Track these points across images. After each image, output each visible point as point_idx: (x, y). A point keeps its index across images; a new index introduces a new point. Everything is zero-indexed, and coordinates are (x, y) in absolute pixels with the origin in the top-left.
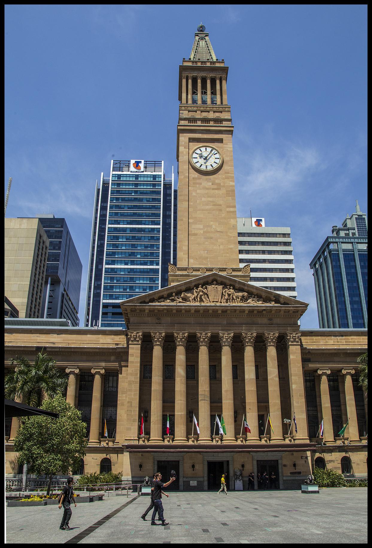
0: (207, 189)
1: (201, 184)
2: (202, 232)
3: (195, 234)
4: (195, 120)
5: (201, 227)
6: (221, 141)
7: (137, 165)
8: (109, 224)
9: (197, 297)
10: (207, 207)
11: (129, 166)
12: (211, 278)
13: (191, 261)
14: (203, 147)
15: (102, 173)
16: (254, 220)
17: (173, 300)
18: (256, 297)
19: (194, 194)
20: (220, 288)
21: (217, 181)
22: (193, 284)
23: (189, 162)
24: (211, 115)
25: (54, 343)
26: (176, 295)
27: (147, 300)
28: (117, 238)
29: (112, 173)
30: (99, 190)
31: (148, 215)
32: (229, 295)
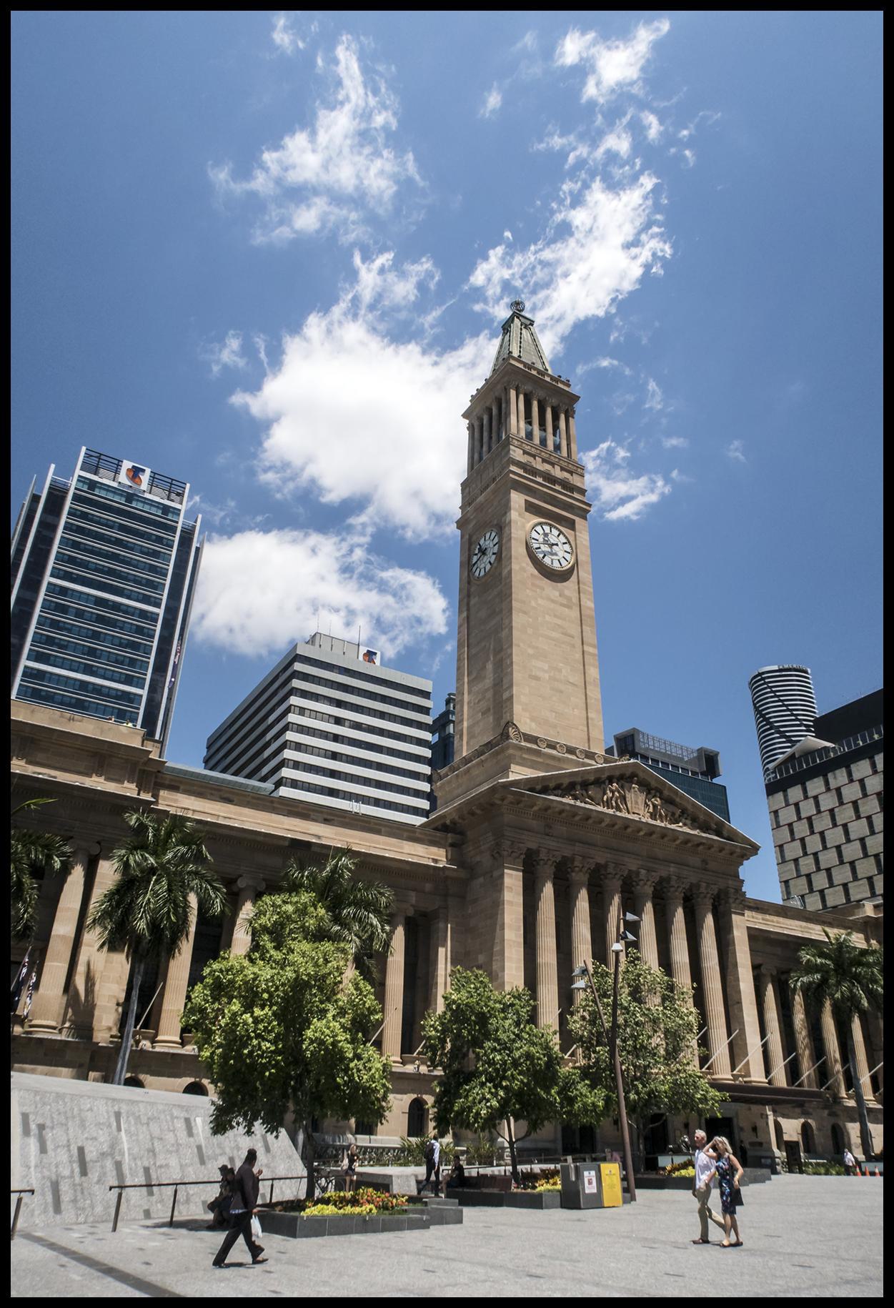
0: (553, 601)
2: (547, 676)
3: (537, 678)
4: (534, 472)
7: (135, 473)
8: (52, 575)
10: (554, 634)
11: (117, 472)
15: (53, 466)
16: (363, 650)
25: (319, 837)
27: (539, 787)
28: (63, 609)
29: (78, 472)
30: (35, 499)
31: (137, 581)
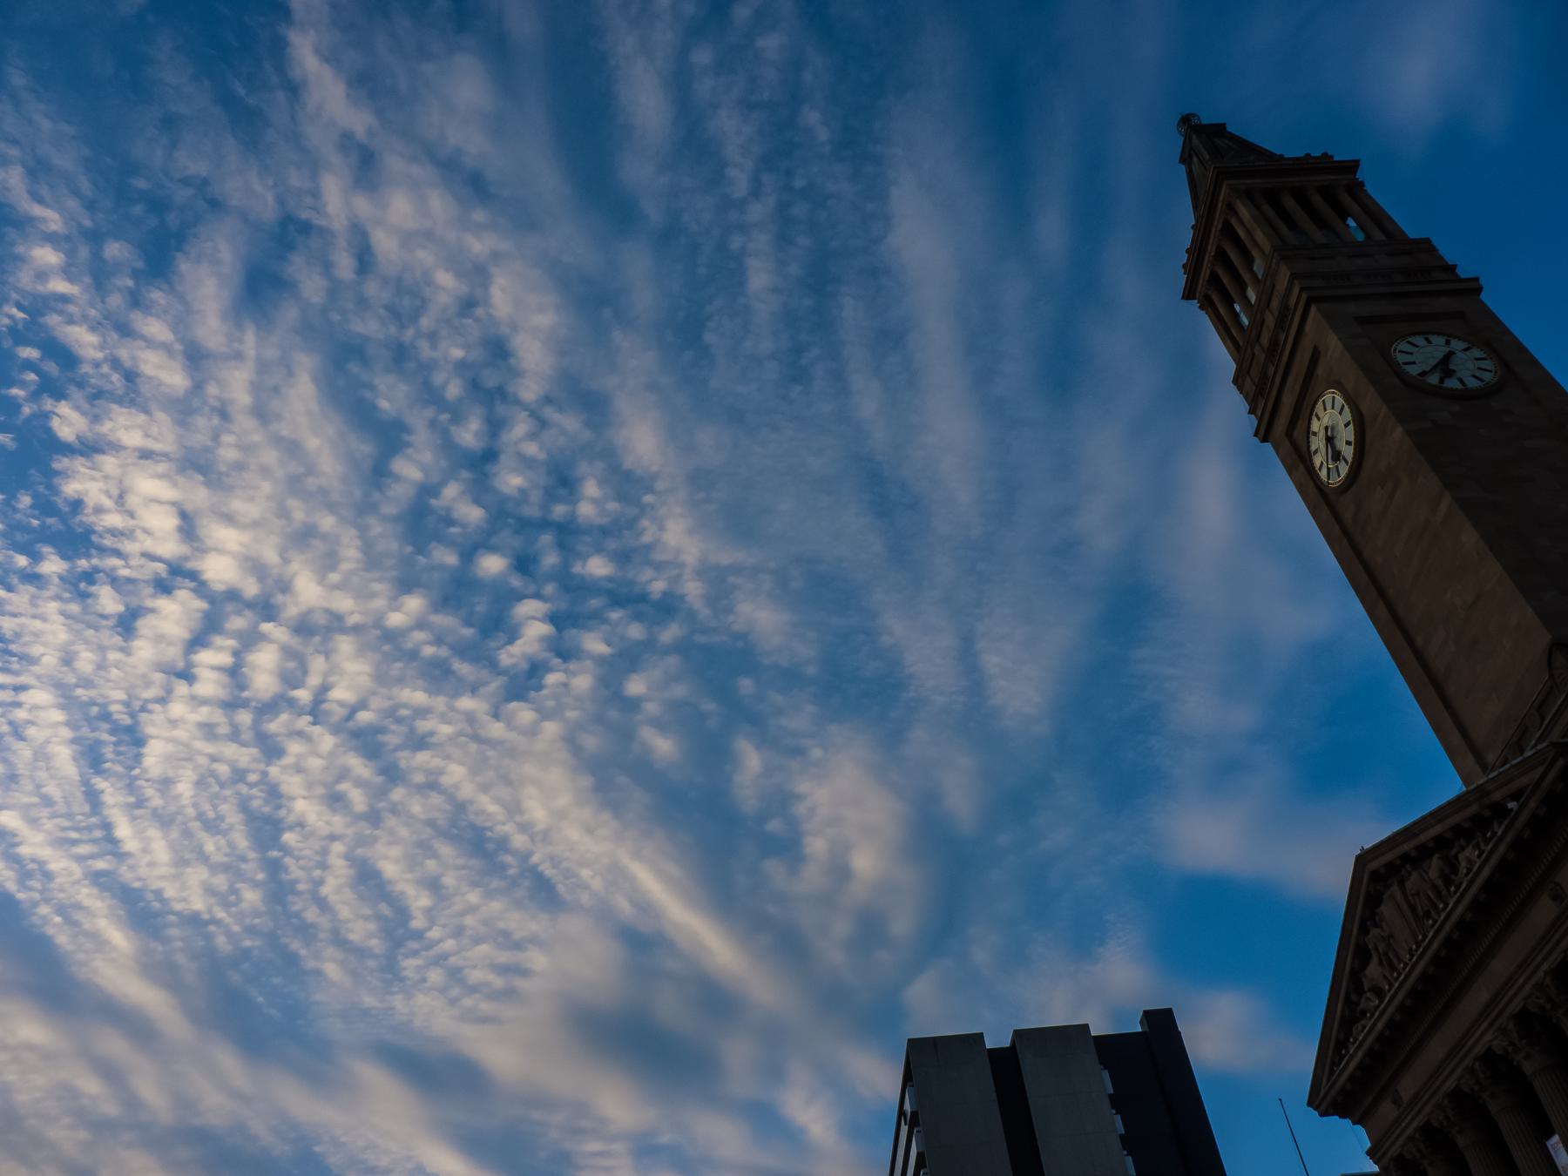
6: (1316, 356)
14: (1310, 419)
17: (1364, 1013)
20: (1395, 889)
24: (1270, 321)
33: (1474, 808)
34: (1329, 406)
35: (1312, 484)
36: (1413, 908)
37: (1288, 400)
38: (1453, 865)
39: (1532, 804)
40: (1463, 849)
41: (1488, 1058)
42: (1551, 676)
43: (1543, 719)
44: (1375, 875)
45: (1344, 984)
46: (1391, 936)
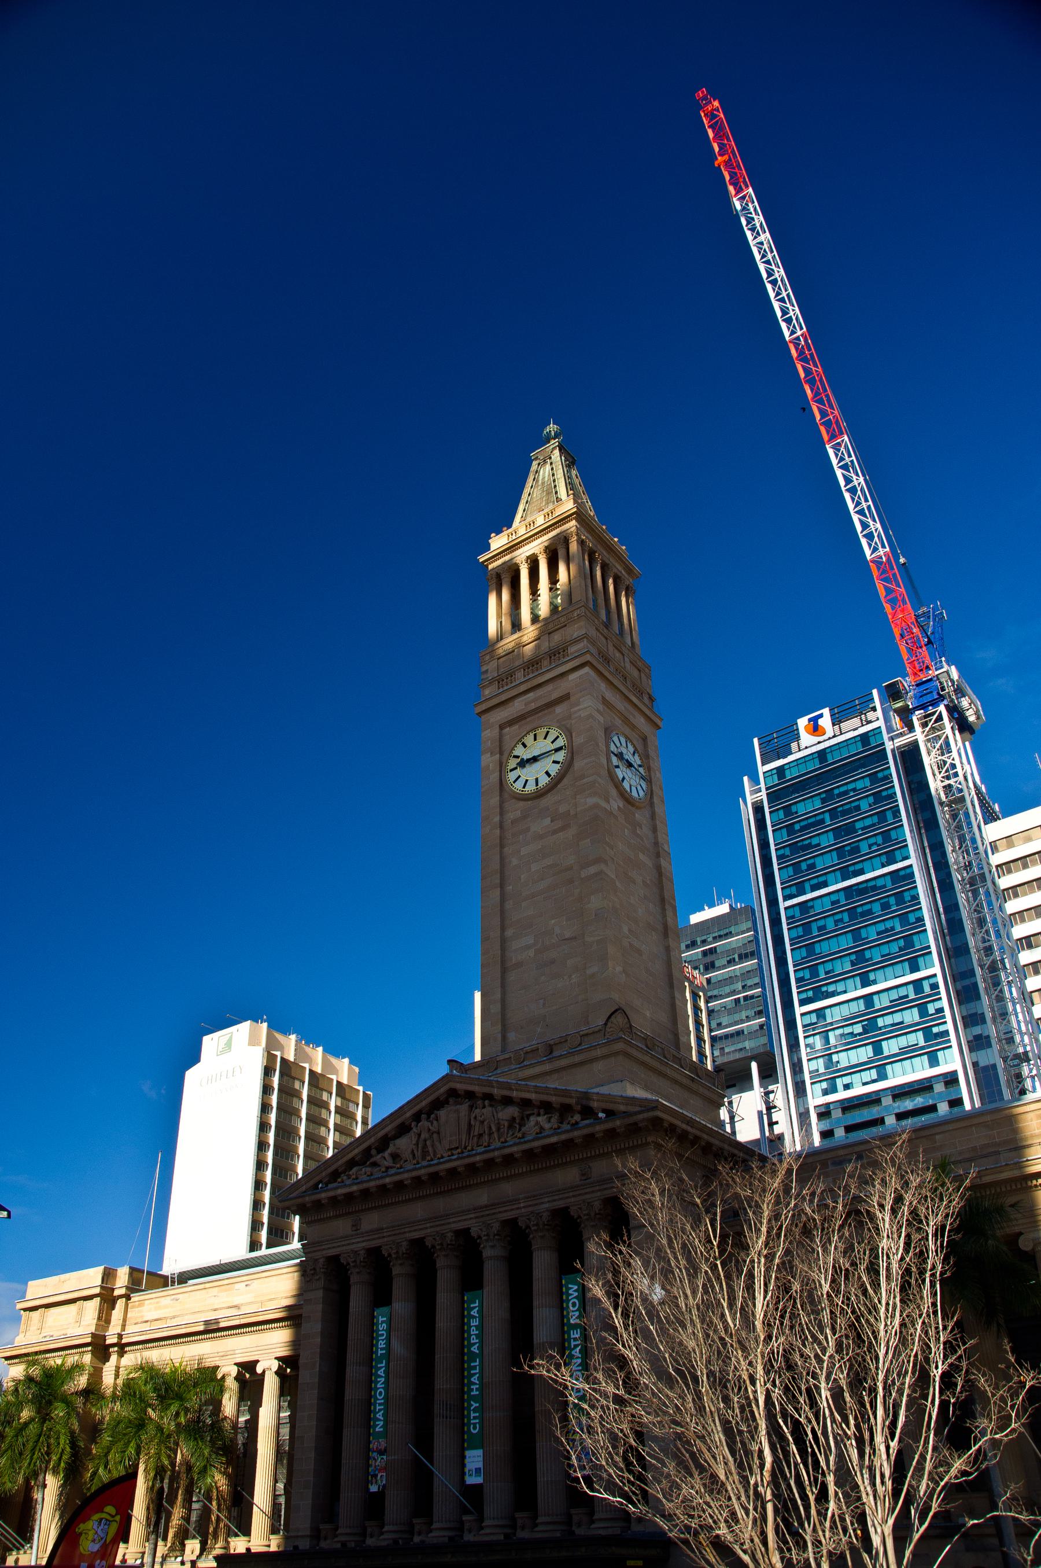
1: (528, 829)
2: (531, 953)
3: (519, 964)
5: (530, 940)
6: (565, 698)
9: (417, 1144)
12: (442, 1090)
13: (512, 1036)
14: (528, 733)
17: (375, 1164)
18: (542, 1111)
19: (515, 862)
20: (464, 1108)
21: (562, 809)
22: (408, 1114)
23: (502, 783)
26: (378, 1153)
32: (482, 1122)
33: (573, 1101)
34: (551, 738)
35: (497, 774)
36: (470, 1125)
37: (518, 707)
38: (524, 1119)
39: (618, 1123)
40: (539, 1115)
41: (464, 1234)
42: (606, 1024)
43: (580, 1045)
44: (453, 1093)
45: (373, 1140)
46: (438, 1133)
